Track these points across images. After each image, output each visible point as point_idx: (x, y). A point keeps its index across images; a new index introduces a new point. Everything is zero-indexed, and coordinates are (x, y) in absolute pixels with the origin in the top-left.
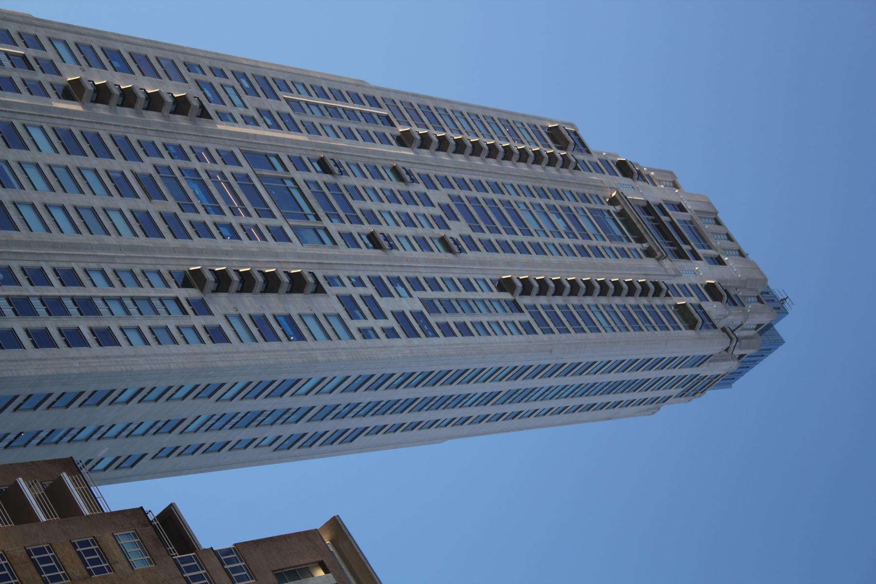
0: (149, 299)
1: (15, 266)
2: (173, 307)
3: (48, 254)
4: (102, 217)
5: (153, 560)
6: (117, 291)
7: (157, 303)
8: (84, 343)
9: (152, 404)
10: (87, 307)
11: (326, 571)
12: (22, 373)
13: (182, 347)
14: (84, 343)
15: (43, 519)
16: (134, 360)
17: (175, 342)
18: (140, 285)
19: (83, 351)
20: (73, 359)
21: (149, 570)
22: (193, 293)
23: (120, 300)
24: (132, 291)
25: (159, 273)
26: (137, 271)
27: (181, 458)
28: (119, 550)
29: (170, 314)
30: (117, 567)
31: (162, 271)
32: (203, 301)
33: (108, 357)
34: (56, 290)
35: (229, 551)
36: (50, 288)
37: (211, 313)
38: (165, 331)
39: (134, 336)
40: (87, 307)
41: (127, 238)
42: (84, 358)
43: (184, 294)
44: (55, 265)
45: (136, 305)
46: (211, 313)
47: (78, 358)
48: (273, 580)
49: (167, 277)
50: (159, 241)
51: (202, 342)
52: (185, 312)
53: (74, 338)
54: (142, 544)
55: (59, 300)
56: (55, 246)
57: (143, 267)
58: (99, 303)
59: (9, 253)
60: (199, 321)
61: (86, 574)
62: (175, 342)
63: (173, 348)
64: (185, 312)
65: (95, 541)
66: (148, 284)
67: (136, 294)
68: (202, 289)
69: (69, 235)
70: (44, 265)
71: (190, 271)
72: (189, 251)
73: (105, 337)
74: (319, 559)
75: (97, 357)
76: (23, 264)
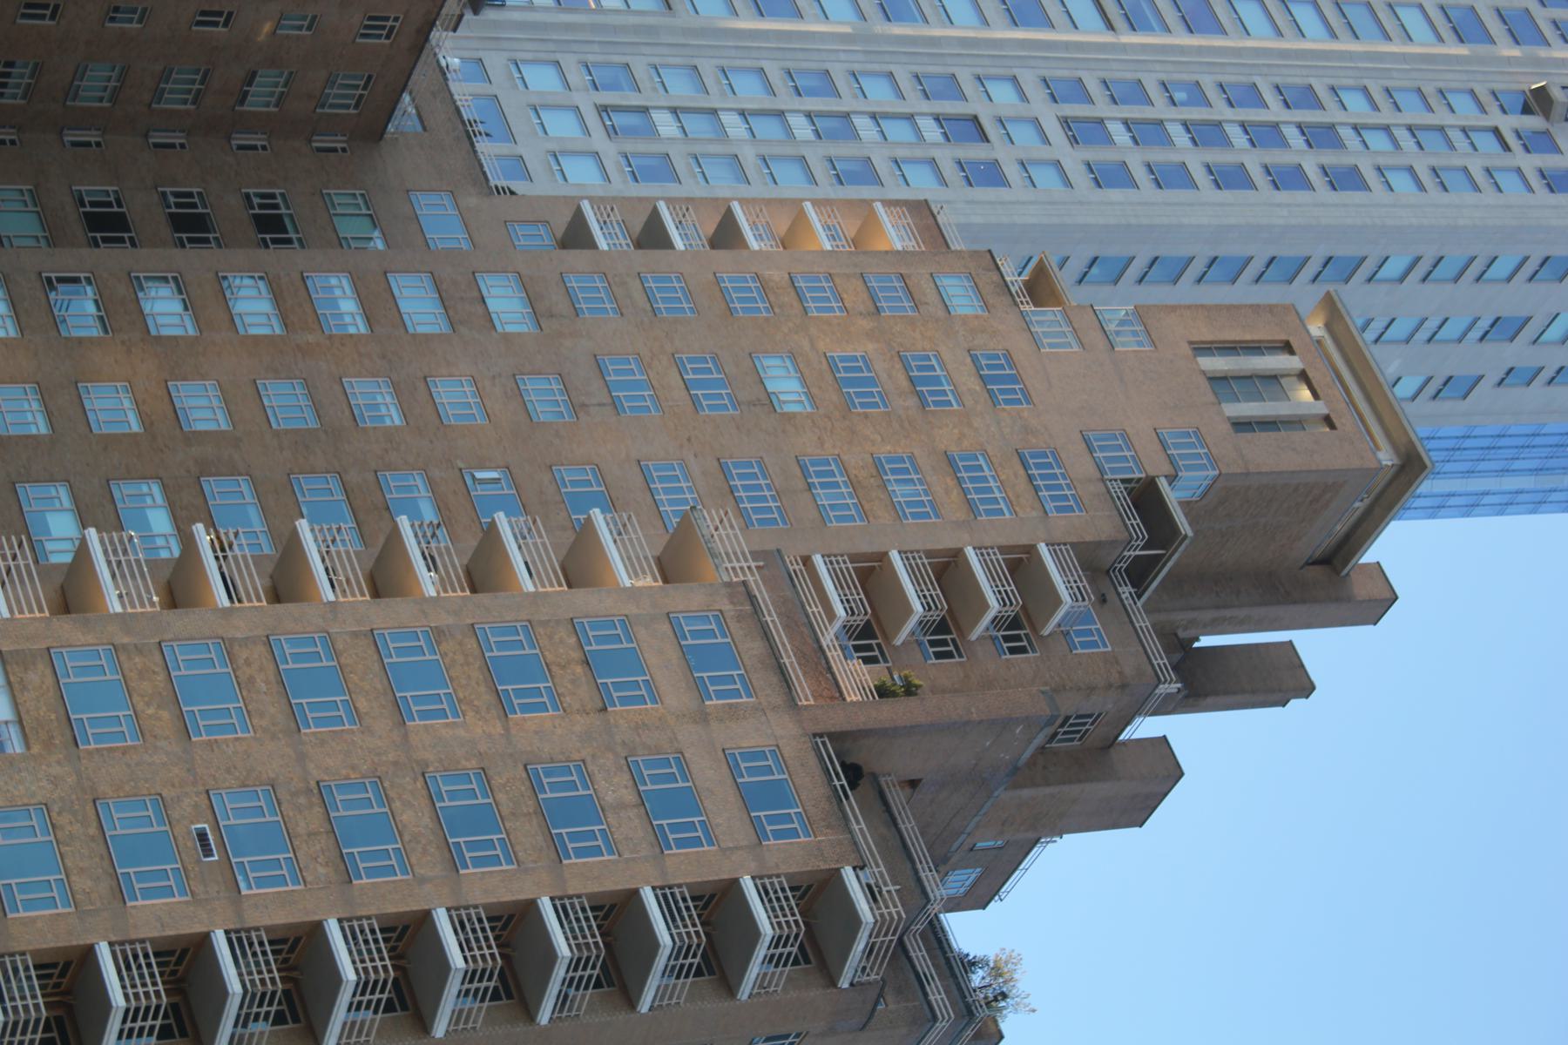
0: (1441, 129)
1: (1208, 83)
2: (1487, 143)
3: (1269, 66)
4: (1384, 15)
6: (1386, 116)
7: (1456, 136)
8: (1307, 185)
9: (1450, 287)
10: (1321, 136)
12: (1185, 221)
13: (1489, 196)
14: (1307, 185)
16: (1396, 209)
17: (1476, 188)
18: (1430, 109)
19: (1302, 196)
20: (1279, 205)
21: (976, 317)
22: (1534, 122)
23: (1386, 129)
24: (1420, 117)
25: (1472, 92)
26: (1428, 90)
27: (1552, 389)
28: (934, 291)
29: (1476, 149)
31: (1478, 89)
32: (1547, 133)
33: (1345, 205)
34: (1274, 111)
36: (1262, 111)
37: (1558, 150)
38: (1461, 176)
39: (1401, 182)
40: (1321, 136)
41: (1423, 43)
42: (1299, 205)
43: (1509, 123)
44: (1278, 80)
45: (1414, 136)
46: (1558, 150)
47: (1288, 205)
48: (1186, 350)
49: (1485, 98)
50: (1483, 49)
51: (1530, 189)
52: (1506, 147)
53: (1287, 179)
55: (1275, 126)
56: (1284, 54)
57: (1441, 85)
58: (1346, 133)
59: (1200, 63)
60: (1530, 163)
61: (872, 309)
62: (1476, 188)
63: (1470, 197)
64: (1506, 147)
66: (1446, 109)
67: (1418, 121)
68: (1547, 115)
69: (1315, 40)
70: (1259, 81)
71: (1532, 91)
72: (1538, 62)
73: (1345, 179)
74: (1283, 337)
75: (1323, 205)
76: (1221, 78)
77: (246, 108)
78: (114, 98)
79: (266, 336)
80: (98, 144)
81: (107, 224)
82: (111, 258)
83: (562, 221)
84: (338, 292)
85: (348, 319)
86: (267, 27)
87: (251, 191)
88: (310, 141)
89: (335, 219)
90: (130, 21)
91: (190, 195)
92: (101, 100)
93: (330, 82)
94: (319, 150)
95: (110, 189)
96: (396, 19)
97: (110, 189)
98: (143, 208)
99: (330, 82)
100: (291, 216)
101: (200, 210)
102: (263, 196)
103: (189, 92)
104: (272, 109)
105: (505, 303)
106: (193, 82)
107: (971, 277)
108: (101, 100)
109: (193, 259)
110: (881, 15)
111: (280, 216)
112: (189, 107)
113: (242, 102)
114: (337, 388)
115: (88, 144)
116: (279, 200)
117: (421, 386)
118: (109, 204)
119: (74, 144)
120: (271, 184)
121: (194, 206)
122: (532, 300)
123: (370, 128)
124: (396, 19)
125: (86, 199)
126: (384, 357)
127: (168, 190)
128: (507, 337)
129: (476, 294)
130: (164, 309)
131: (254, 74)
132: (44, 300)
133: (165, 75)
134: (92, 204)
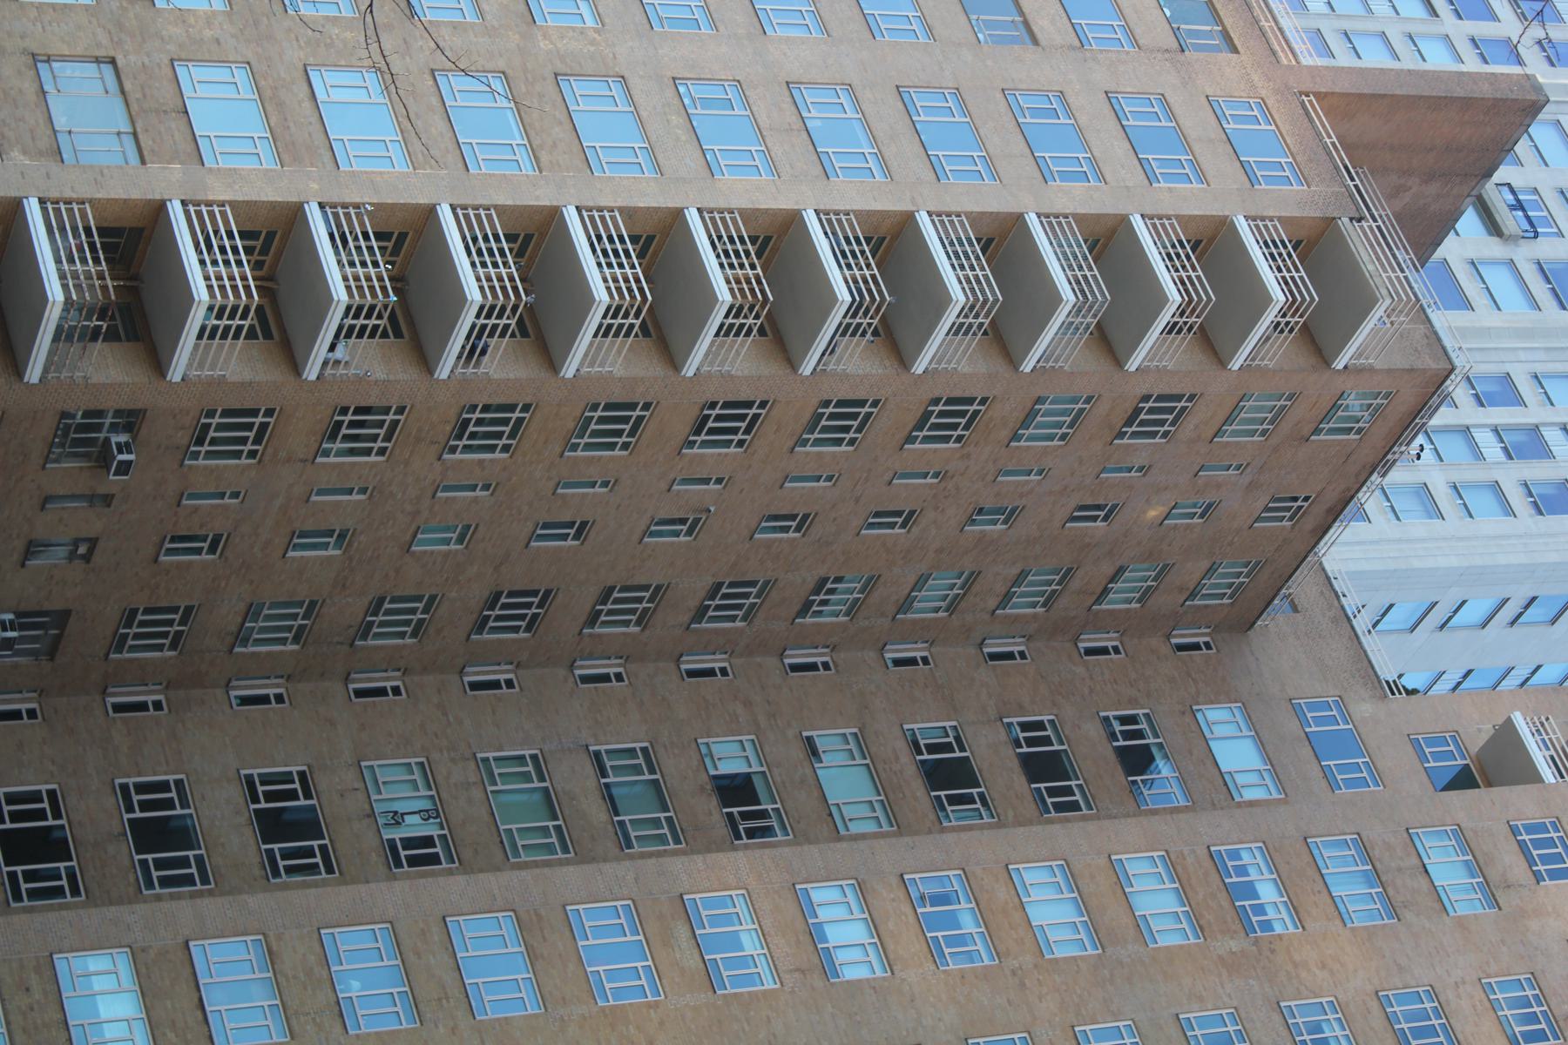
77: (1104, 607)
78: (952, 608)
79: (1181, 947)
80: (925, 661)
81: (949, 775)
82: (973, 840)
83: (1478, 735)
84: (1253, 875)
85: (1271, 914)
86: (1153, 514)
87: (1111, 714)
88: (1168, 637)
89: (1211, 743)
90: (995, 522)
91: (1039, 726)
92: (937, 610)
93: (1211, 571)
94: (1181, 648)
95: (947, 724)
96: (1306, 499)
97: (947, 724)
98: (995, 757)
99: (1211, 571)
100: (1160, 746)
101: (1056, 747)
102: (1124, 720)
103: (1042, 594)
104: (1134, 605)
105: (1447, 869)
106: (1049, 583)
108: (937, 610)
109: (1068, 834)
110: (1554, 303)
111: (1147, 746)
112: (1039, 610)
113: (1098, 601)
114: (1277, 1018)
115: (912, 662)
116: (1144, 726)
117: (1374, 1004)
118: (947, 747)
119: (898, 662)
120: (1133, 702)
121: (1046, 741)
122: (1477, 867)
123: (1242, 618)
124: (1306, 499)
125: (922, 742)
126: (1324, 966)
127: (1015, 720)
128: (1461, 923)
129: (1415, 861)
130: (1051, 910)
131: (1121, 570)
132: (911, 919)
133: (1020, 579)
134: (932, 749)
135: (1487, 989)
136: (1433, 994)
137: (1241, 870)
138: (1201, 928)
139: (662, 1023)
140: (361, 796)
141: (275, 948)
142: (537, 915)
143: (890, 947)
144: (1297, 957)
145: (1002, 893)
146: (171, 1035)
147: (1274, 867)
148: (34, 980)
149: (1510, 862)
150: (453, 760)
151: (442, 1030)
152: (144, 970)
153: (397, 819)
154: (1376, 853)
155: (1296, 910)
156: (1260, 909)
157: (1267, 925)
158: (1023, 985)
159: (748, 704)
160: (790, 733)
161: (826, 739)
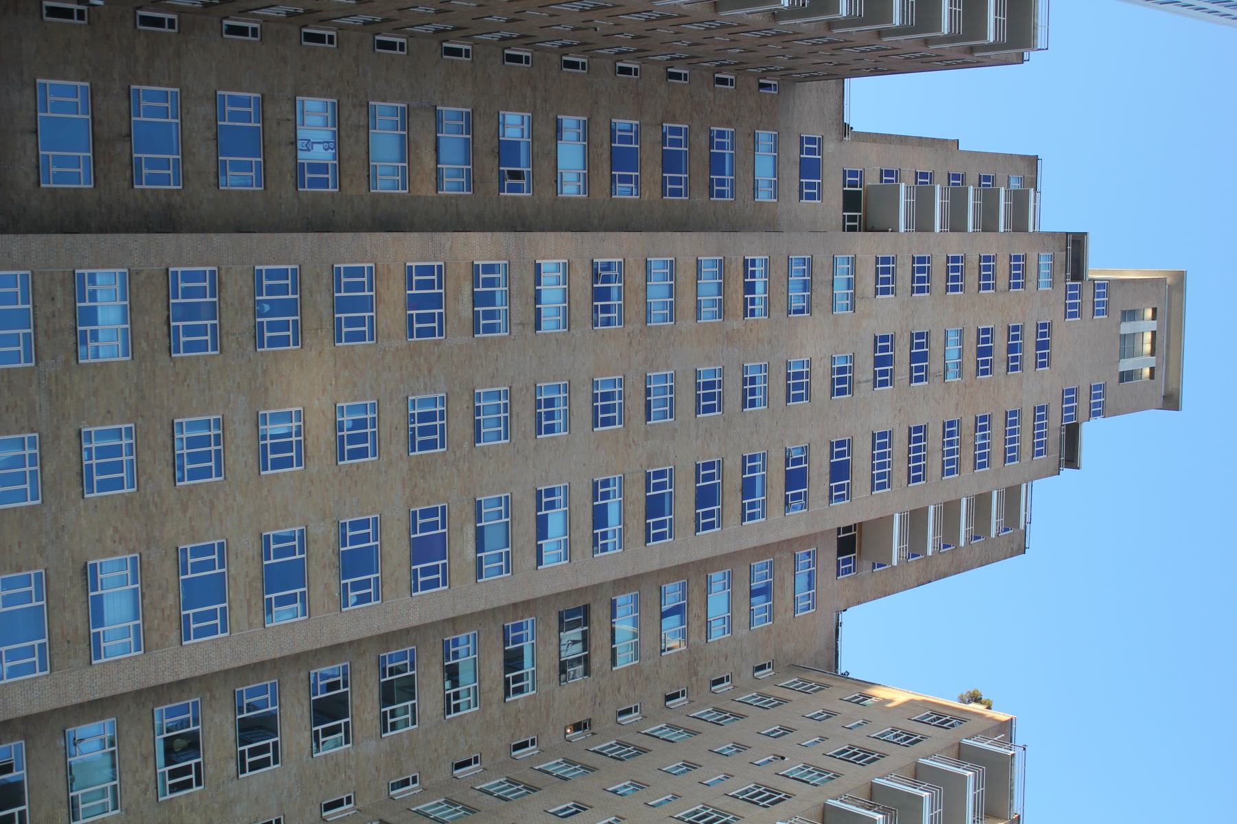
5: (1052, 284)
11: (1154, 318)
15: (1002, 229)
30: (1029, 285)
35: (1101, 286)
54: (1052, 267)
65: (1025, 258)
107: (1053, 258)
120: (729, 124)
126: (770, 342)
135: (833, 359)
136: (809, 363)
137: (753, 274)
138: (722, 312)
139: (439, 357)
140: (291, 125)
141: (224, 280)
142: (389, 269)
143: (573, 311)
144: (760, 335)
145: (639, 278)
146: (144, 345)
147: (767, 274)
148: (58, 293)
149: (867, 282)
150: (354, 106)
151: (313, 352)
152: (135, 291)
153: (310, 145)
154: (815, 270)
155: (768, 302)
156: (753, 301)
157: (753, 313)
158: (631, 343)
159: (534, 89)
160: (551, 116)
161: (570, 122)
